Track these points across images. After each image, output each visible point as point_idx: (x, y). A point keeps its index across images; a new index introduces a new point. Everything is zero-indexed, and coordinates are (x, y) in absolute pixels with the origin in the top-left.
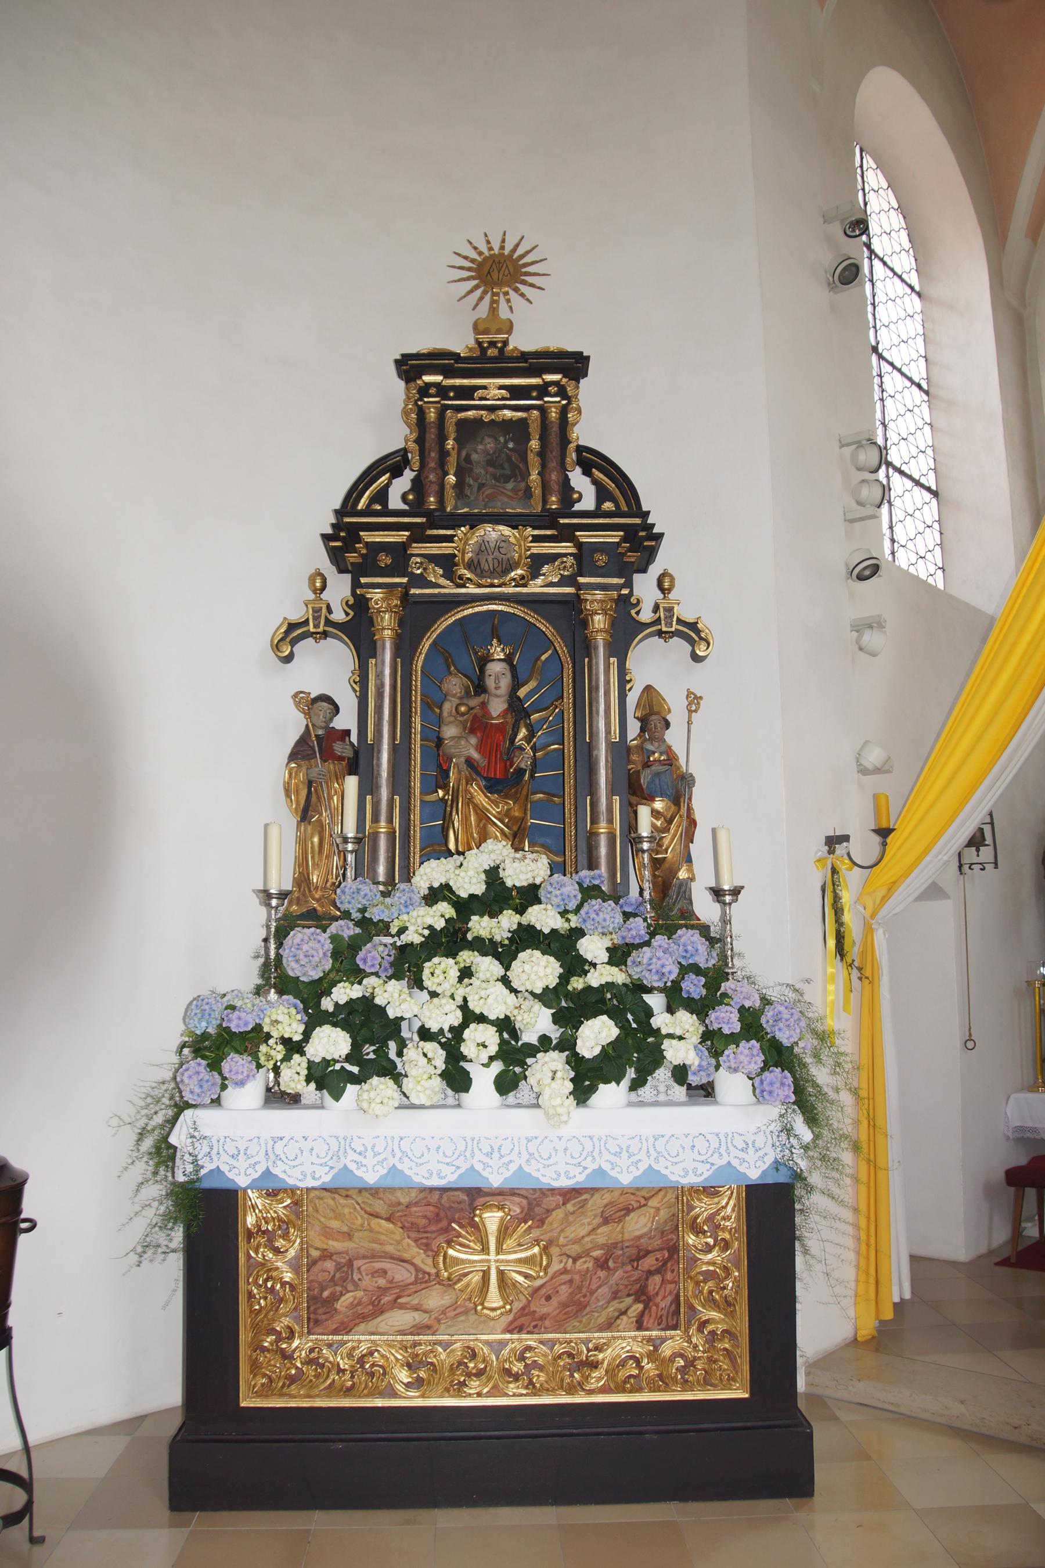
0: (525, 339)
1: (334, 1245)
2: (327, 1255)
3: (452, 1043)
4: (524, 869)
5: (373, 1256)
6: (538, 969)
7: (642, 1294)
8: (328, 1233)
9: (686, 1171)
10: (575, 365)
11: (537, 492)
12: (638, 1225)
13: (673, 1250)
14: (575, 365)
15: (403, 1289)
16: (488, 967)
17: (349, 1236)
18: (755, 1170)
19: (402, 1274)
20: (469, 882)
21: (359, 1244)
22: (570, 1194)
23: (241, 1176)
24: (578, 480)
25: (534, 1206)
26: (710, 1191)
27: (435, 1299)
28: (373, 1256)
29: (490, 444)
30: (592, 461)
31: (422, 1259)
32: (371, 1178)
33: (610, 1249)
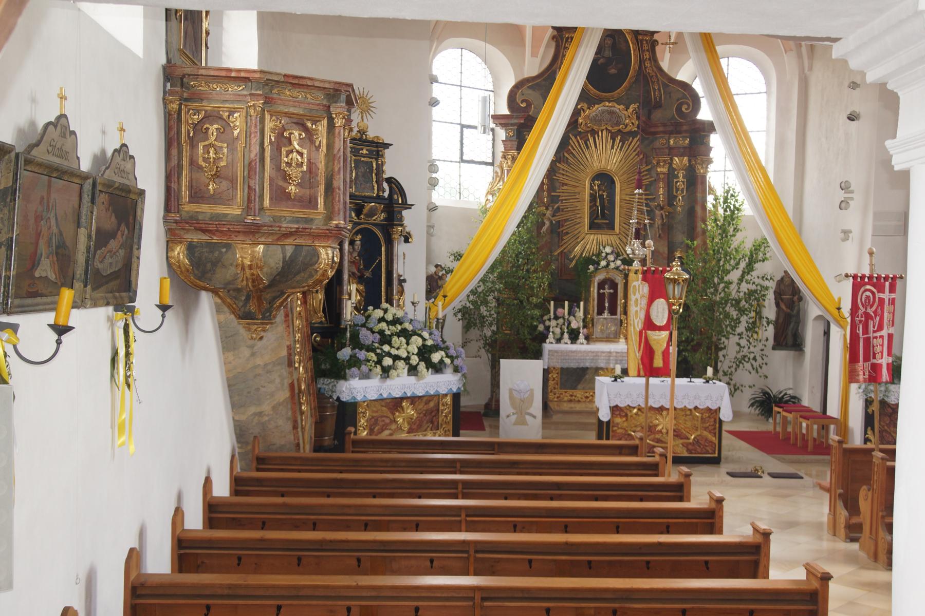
0: (371, 135)
1: (375, 415)
2: (373, 417)
3: (407, 360)
4: (400, 314)
5: (382, 417)
6: (416, 341)
7: (432, 422)
8: (373, 412)
9: (443, 390)
10: (387, 146)
12: (432, 404)
13: (438, 410)
14: (387, 146)
15: (387, 425)
16: (403, 339)
17: (377, 412)
18: (455, 390)
19: (387, 421)
20: (389, 317)
21: (379, 414)
22: (420, 397)
23: (359, 398)
24: (385, 185)
25: (414, 400)
26: (446, 395)
27: (394, 427)
28: (382, 417)
30: (390, 180)
31: (391, 417)
32: (385, 396)
33: (426, 411)
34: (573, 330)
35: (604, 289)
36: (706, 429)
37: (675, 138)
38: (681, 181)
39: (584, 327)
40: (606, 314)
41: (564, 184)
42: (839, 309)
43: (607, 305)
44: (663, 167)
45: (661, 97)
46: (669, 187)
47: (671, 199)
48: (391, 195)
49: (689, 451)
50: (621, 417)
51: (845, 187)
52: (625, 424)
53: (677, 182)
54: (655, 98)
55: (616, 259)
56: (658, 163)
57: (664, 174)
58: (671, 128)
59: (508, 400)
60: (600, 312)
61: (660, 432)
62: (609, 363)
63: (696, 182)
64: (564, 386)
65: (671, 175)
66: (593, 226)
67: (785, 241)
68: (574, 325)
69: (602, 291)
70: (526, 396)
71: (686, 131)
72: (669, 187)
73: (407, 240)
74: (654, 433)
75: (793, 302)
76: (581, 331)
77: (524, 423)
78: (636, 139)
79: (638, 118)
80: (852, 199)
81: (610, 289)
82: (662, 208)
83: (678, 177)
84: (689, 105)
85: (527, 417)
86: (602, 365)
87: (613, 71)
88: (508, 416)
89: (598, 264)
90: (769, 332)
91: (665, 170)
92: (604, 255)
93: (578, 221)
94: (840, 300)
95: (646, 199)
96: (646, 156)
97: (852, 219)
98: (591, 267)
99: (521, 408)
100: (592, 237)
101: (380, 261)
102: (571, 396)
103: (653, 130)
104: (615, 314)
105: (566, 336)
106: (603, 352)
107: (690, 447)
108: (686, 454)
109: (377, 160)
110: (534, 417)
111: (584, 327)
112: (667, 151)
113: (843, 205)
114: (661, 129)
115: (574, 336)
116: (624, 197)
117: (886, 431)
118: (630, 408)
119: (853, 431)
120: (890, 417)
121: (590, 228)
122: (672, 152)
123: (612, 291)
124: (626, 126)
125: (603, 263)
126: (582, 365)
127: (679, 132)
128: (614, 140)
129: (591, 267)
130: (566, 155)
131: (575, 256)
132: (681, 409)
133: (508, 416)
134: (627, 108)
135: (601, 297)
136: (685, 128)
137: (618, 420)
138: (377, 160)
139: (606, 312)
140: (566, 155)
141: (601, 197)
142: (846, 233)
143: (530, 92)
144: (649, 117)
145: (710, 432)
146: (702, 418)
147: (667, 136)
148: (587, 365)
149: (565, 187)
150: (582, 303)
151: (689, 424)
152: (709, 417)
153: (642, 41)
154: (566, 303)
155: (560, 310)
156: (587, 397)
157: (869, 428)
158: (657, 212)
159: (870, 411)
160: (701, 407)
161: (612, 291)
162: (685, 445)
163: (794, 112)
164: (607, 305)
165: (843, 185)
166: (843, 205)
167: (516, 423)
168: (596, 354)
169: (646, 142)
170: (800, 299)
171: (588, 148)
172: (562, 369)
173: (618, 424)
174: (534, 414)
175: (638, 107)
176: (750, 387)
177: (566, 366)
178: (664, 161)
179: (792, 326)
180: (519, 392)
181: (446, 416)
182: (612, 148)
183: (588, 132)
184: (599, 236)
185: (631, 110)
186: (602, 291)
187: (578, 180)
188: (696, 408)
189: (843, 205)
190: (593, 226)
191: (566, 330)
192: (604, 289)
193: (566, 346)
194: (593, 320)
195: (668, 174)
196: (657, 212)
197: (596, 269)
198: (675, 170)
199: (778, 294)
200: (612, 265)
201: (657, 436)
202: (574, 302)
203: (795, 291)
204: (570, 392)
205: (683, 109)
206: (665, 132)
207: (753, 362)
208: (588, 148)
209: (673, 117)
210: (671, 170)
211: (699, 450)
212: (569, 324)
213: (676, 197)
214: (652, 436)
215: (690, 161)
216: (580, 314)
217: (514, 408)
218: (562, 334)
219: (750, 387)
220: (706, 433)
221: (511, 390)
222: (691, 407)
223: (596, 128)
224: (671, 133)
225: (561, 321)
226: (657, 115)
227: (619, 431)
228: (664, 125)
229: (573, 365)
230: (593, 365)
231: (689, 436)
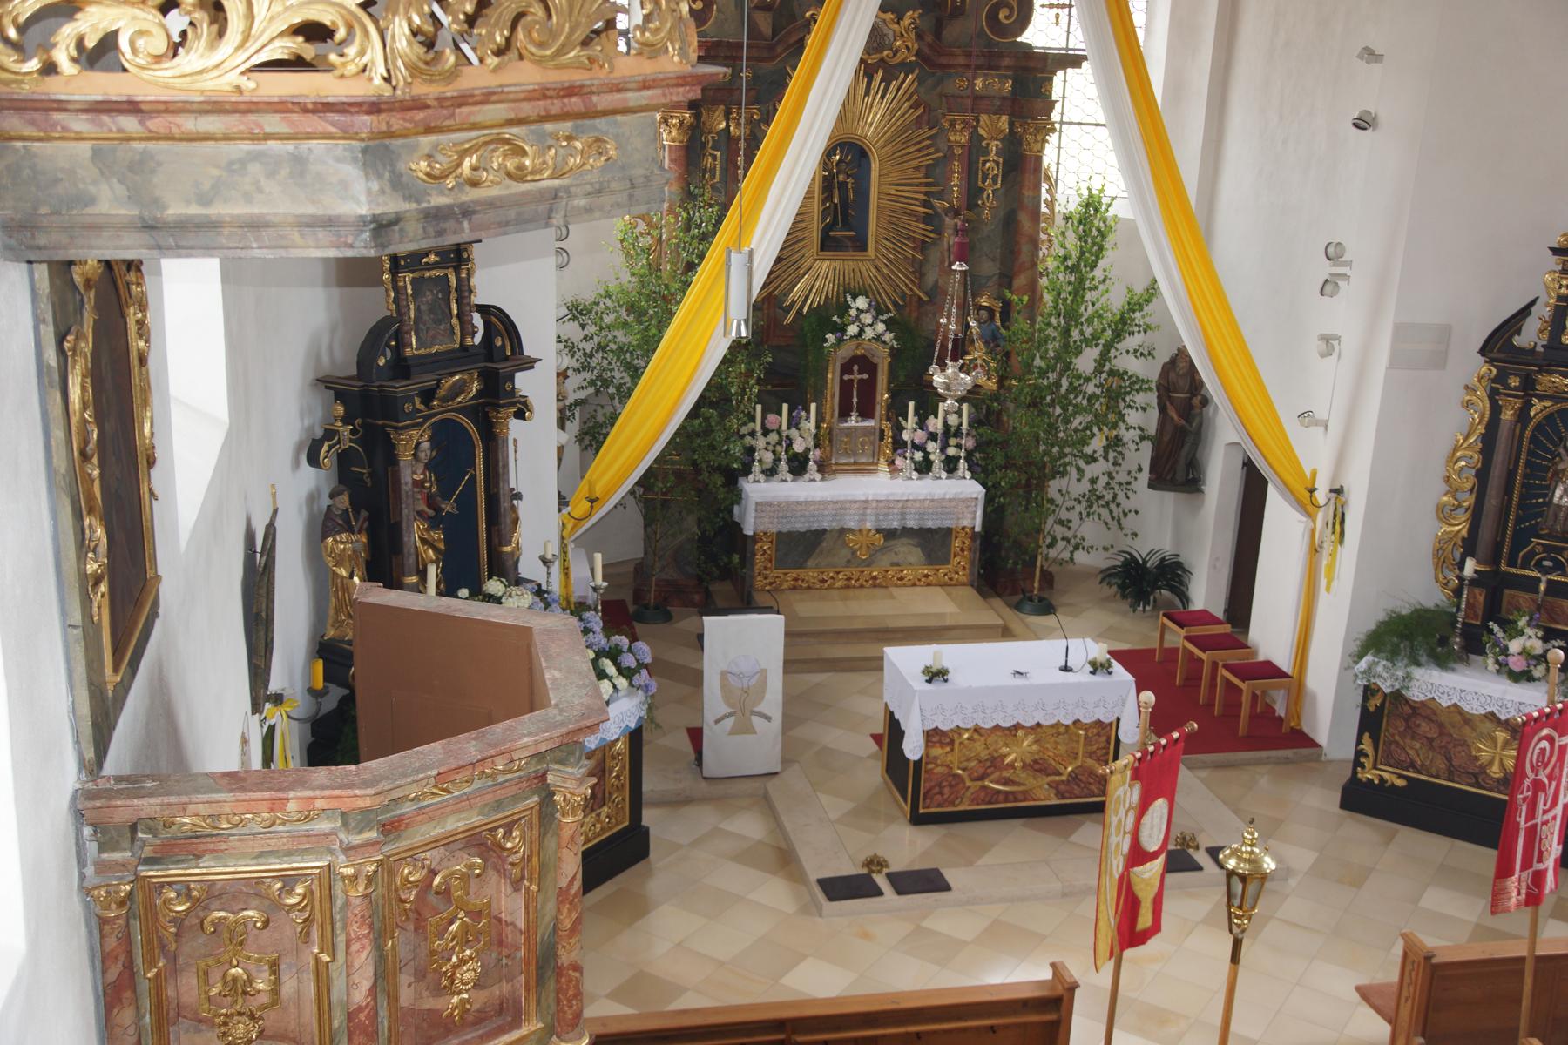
11: (457, 329)
24: (478, 320)
29: (429, 297)
34: (796, 454)
35: (851, 373)
36: (1090, 755)
37: (986, 77)
38: (992, 164)
39: (817, 446)
42: (1312, 491)
43: (855, 400)
44: (961, 131)
46: (971, 171)
48: (487, 337)
49: (1060, 795)
50: (942, 745)
51: (1333, 254)
52: (950, 757)
53: (984, 163)
55: (875, 319)
56: (952, 124)
57: (962, 146)
58: (981, 61)
59: (718, 692)
60: (844, 414)
61: (1011, 765)
62: (863, 520)
63: (1022, 166)
64: (781, 563)
65: (975, 148)
67: (1225, 363)
68: (798, 447)
69: (846, 377)
70: (753, 681)
71: (1008, 68)
72: (971, 171)
73: (520, 415)
74: (1001, 769)
75: (1191, 407)
76: (811, 456)
77: (749, 730)
79: (919, 37)
80: (1344, 277)
82: (957, 213)
84: (1011, 9)
85: (756, 720)
86: (852, 525)
88: (717, 721)
89: (843, 330)
90: (1142, 455)
91: (963, 139)
92: (853, 312)
94: (1314, 474)
95: (926, 193)
96: (929, 110)
97: (1343, 315)
98: (829, 336)
99: (743, 706)
100: (826, 264)
101: (474, 478)
102: (796, 580)
103: (944, 61)
105: (783, 466)
106: (854, 502)
107: (1062, 787)
108: (1055, 801)
109: (457, 270)
110: (768, 718)
111: (817, 446)
113: (1328, 287)
114: (961, 60)
115: (798, 466)
116: (886, 189)
117: (1397, 744)
118: (958, 730)
119: (1314, 698)
120: (1406, 720)
121: (823, 247)
122: (978, 103)
123: (865, 376)
125: (852, 329)
126: (815, 526)
127: (997, 68)
129: (829, 336)
131: (793, 304)
132: (1052, 726)
133: (717, 721)
134: (900, 19)
135: (846, 388)
136: (1007, 62)
137: (937, 751)
138: (457, 270)
141: (843, 185)
142: (1329, 342)
144: (938, 34)
145: (1098, 760)
146: (1086, 738)
147: (969, 73)
148: (826, 525)
150: (813, 406)
151: (1062, 749)
152: (1098, 734)
154: (785, 407)
155: (771, 417)
156: (824, 581)
157: (1366, 735)
158: (949, 221)
159: (1372, 709)
160: (1084, 721)
161: (865, 376)
162: (1054, 786)
163: (1209, 36)
164: (855, 400)
165: (1331, 250)
166: (1328, 287)
167: (734, 731)
168: (841, 506)
169: (930, 81)
170: (1206, 401)
172: (779, 533)
173: (936, 758)
174: (768, 713)
175: (920, 16)
176: (1105, 549)
177: (786, 528)
179: (1186, 448)
180: (739, 676)
181: (618, 777)
182: (867, 93)
185: (907, 21)
188: (1076, 722)
189: (1328, 288)
191: (784, 457)
192: (851, 373)
193: (787, 489)
196: (949, 221)
197: (840, 341)
199: (1165, 388)
200: (869, 333)
201: (1006, 774)
202: (799, 403)
203: (1196, 385)
204: (794, 573)
205: (1001, 16)
207: (1113, 506)
209: (981, 33)
210: (976, 138)
211: (1077, 791)
212: (790, 445)
213: (983, 190)
214: (997, 775)
215: (1011, 124)
216: (810, 425)
217: (727, 702)
218: (777, 460)
219: (1105, 549)
220: (1090, 762)
221: (724, 674)
222: (1069, 722)
224: (979, 67)
225: (773, 437)
226: (953, 31)
227: (940, 770)
228: (968, 55)
229: (800, 527)
230: (835, 525)
231: (1061, 769)
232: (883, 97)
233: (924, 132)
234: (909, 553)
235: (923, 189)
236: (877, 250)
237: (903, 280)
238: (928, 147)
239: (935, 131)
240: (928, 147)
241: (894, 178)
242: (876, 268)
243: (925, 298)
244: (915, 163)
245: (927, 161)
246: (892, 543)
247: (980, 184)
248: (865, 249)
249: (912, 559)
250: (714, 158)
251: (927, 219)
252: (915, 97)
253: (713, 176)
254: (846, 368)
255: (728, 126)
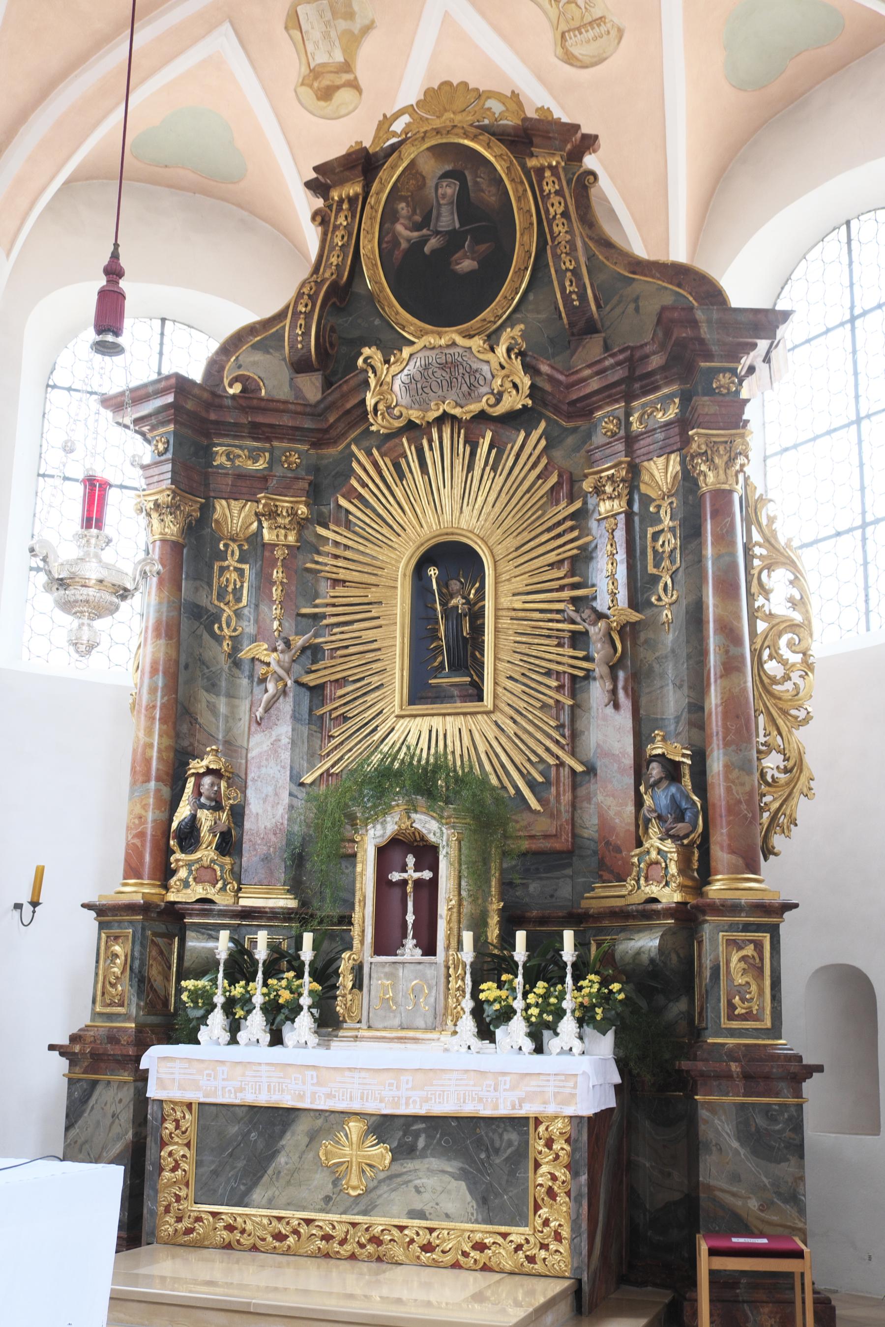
40: (410, 950)
41: (336, 582)
43: (410, 918)
45: (583, 296)
47: (640, 589)
53: (656, 536)
54: (566, 298)
66: (421, 693)
78: (535, 435)
81: (418, 868)
83: (660, 521)
87: (466, 265)
93: (375, 680)
104: (434, 953)
112: (620, 447)
114: (595, 385)
121: (414, 699)
124: (499, 397)
128: (473, 444)
130: (343, 502)
139: (410, 942)
140: (343, 502)
143: (258, 357)
149: (340, 590)
153: (540, 171)
164: (410, 918)
169: (570, 441)
171: (401, 476)
178: (611, 478)
182: (470, 468)
183: (400, 432)
184: (437, 722)
186: (395, 876)
187: (377, 567)
190: (421, 693)
194: (358, 970)
195: (629, 516)
198: (646, 500)
206: (607, 394)
208: (401, 476)
213: (656, 579)
223: (415, 415)
232: (494, 469)
233: (564, 509)
234: (440, 1188)
235: (567, 594)
236: (496, 696)
237: (545, 743)
238: (572, 529)
239: (578, 505)
240: (572, 529)
241: (519, 584)
242: (496, 723)
243: (579, 768)
244: (552, 557)
245: (571, 550)
246: (410, 1165)
247: (651, 570)
248: (481, 699)
249: (450, 1207)
250: (240, 572)
251: (578, 639)
252: (544, 461)
253: (238, 600)
254: (386, 854)
255: (260, 526)
